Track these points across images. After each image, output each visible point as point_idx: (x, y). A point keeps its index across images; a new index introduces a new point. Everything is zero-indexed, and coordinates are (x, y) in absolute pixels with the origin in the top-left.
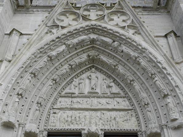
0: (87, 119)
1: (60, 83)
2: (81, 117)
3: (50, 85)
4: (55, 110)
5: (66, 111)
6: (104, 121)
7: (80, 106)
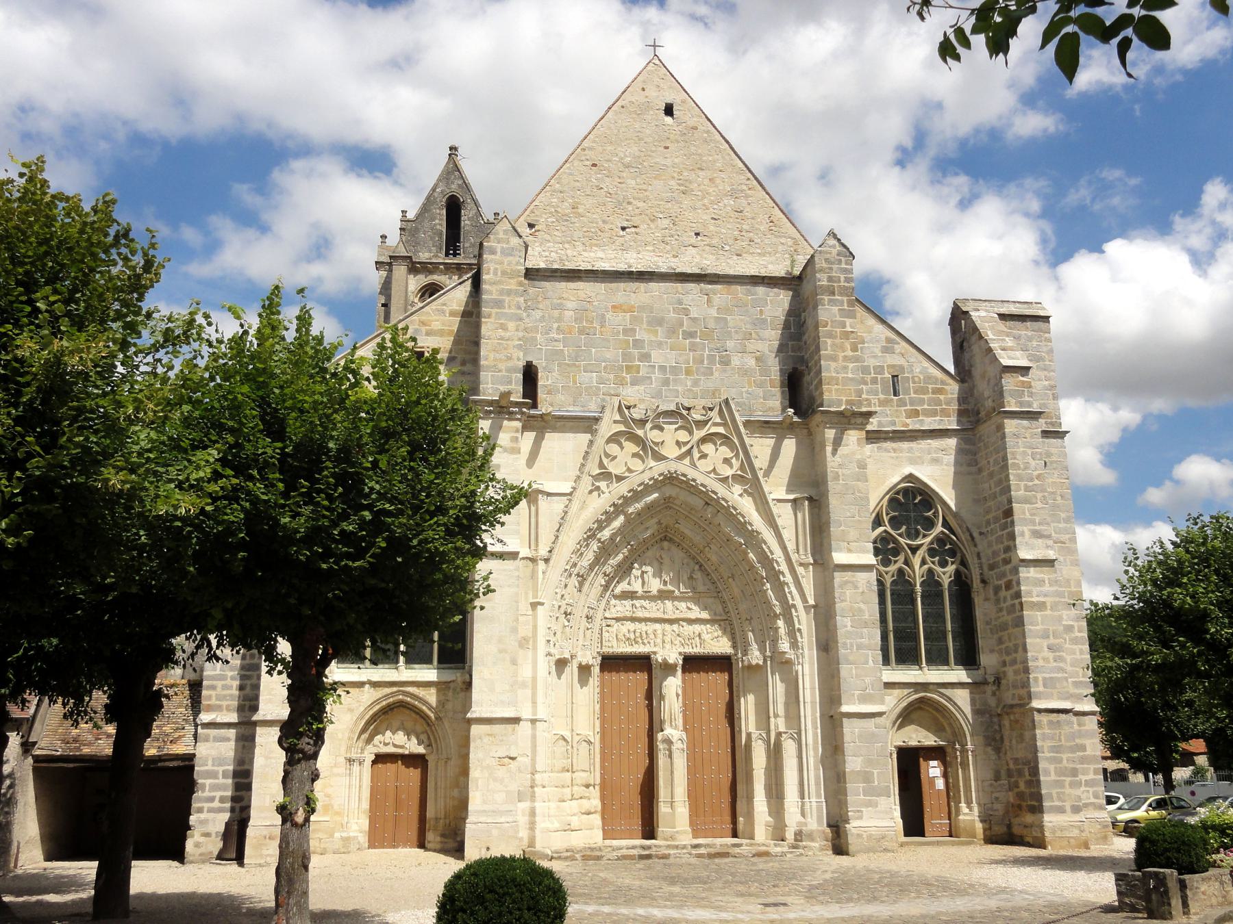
4: (609, 622)
7: (648, 615)
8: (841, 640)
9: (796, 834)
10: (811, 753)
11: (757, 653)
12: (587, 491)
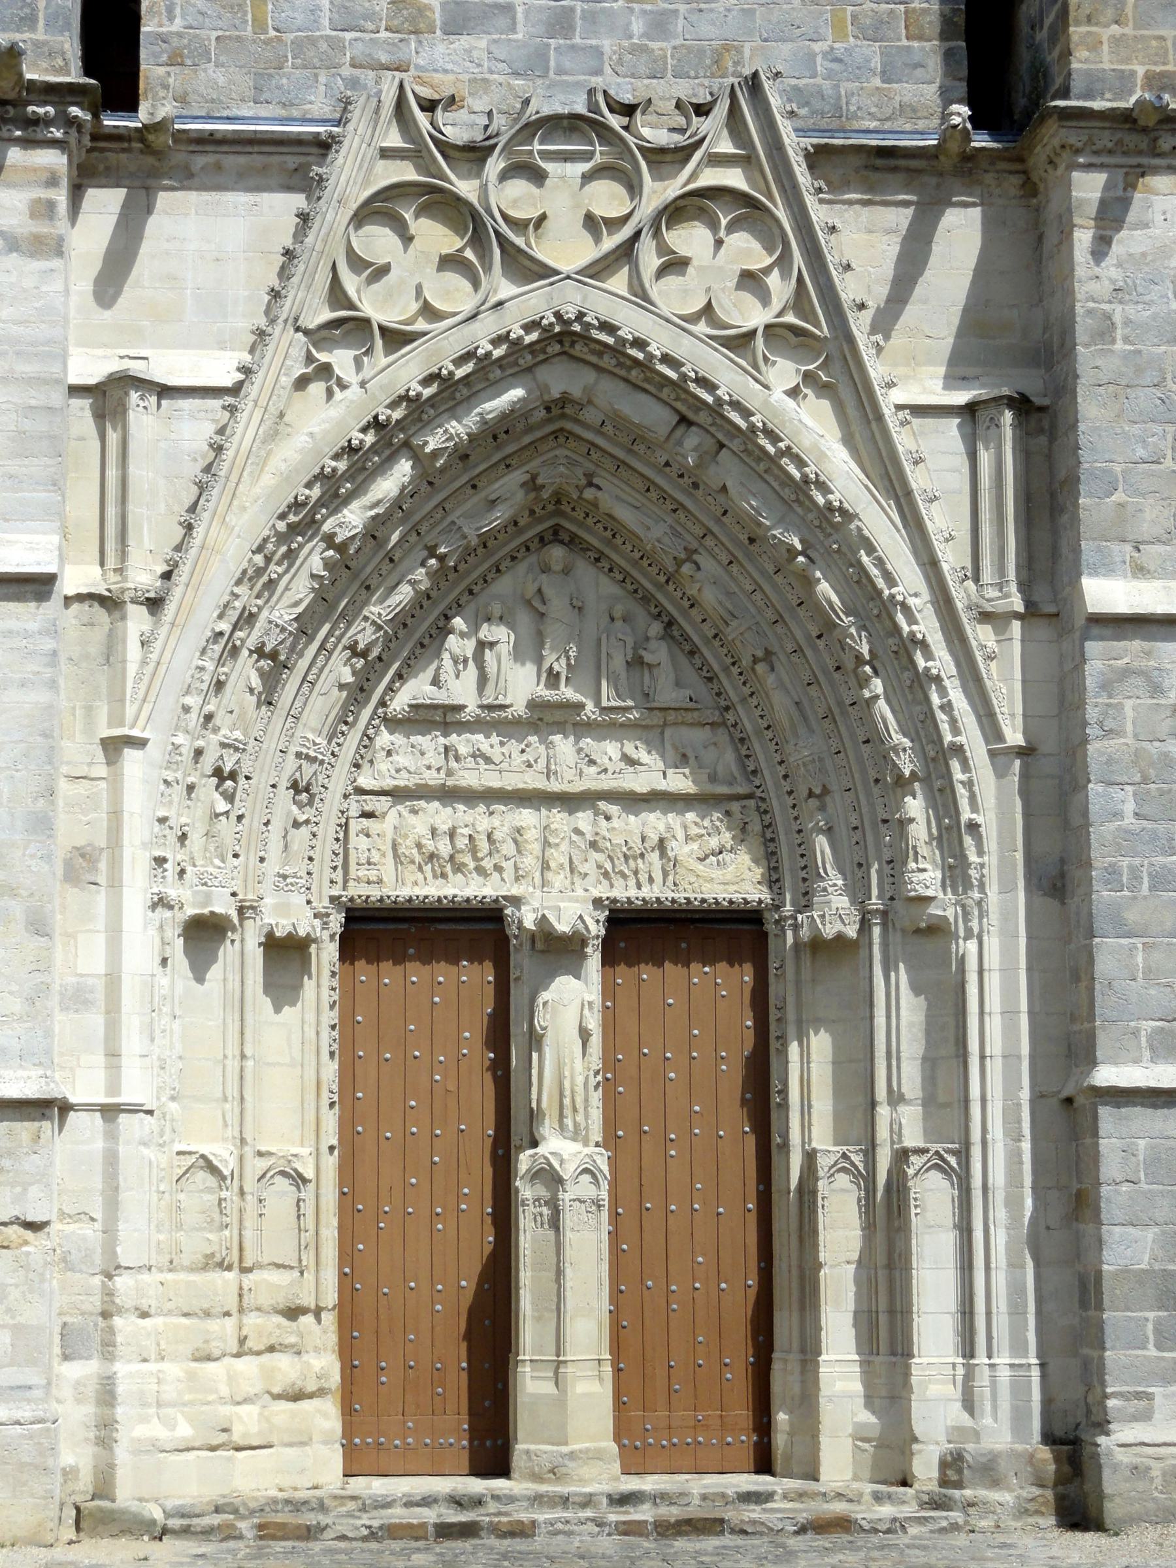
0: (529, 847)
2: (497, 835)
7: (493, 781)
8: (1100, 858)
9: (944, 1465)
10: (1000, 1213)
11: (841, 902)
12: (287, 381)
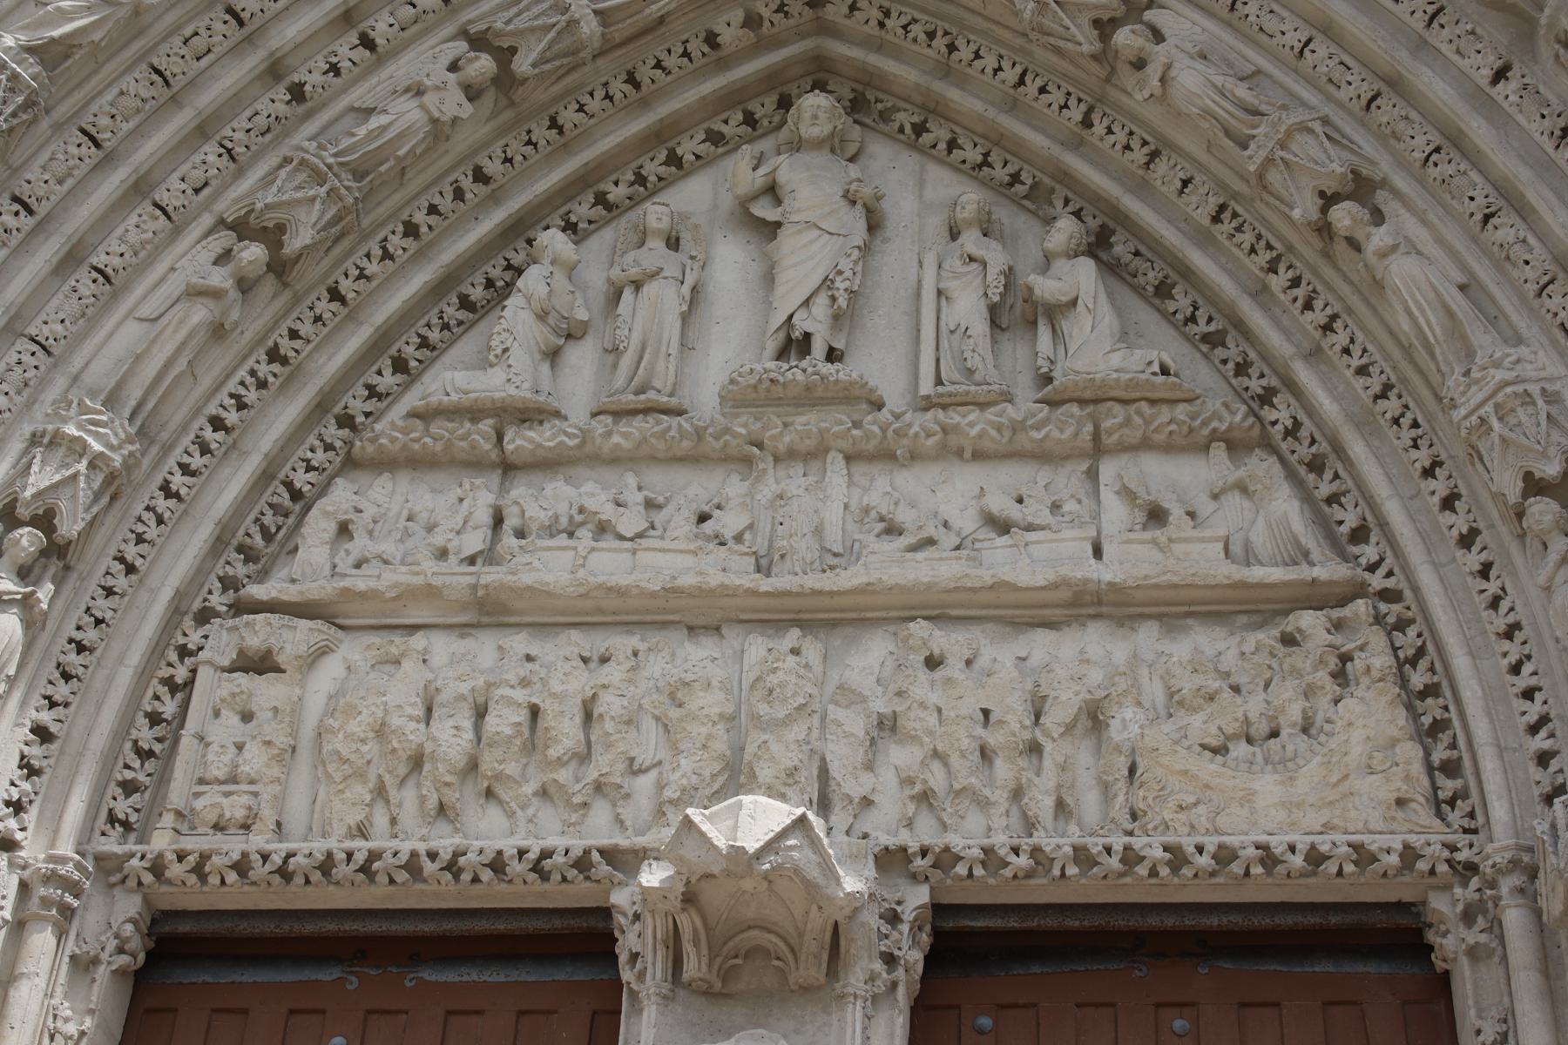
1: (345, 286)
2: (610, 704)
3: (196, 293)
4: (259, 632)
5: (418, 641)
6: (936, 754)
